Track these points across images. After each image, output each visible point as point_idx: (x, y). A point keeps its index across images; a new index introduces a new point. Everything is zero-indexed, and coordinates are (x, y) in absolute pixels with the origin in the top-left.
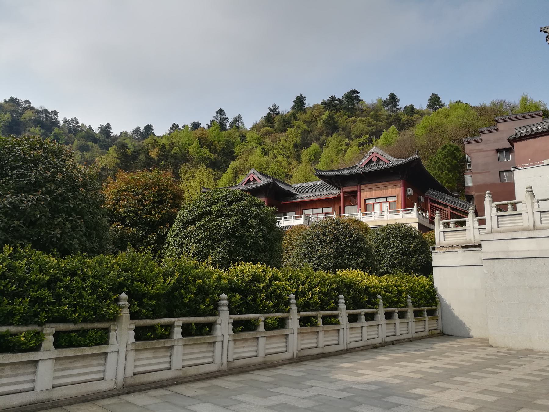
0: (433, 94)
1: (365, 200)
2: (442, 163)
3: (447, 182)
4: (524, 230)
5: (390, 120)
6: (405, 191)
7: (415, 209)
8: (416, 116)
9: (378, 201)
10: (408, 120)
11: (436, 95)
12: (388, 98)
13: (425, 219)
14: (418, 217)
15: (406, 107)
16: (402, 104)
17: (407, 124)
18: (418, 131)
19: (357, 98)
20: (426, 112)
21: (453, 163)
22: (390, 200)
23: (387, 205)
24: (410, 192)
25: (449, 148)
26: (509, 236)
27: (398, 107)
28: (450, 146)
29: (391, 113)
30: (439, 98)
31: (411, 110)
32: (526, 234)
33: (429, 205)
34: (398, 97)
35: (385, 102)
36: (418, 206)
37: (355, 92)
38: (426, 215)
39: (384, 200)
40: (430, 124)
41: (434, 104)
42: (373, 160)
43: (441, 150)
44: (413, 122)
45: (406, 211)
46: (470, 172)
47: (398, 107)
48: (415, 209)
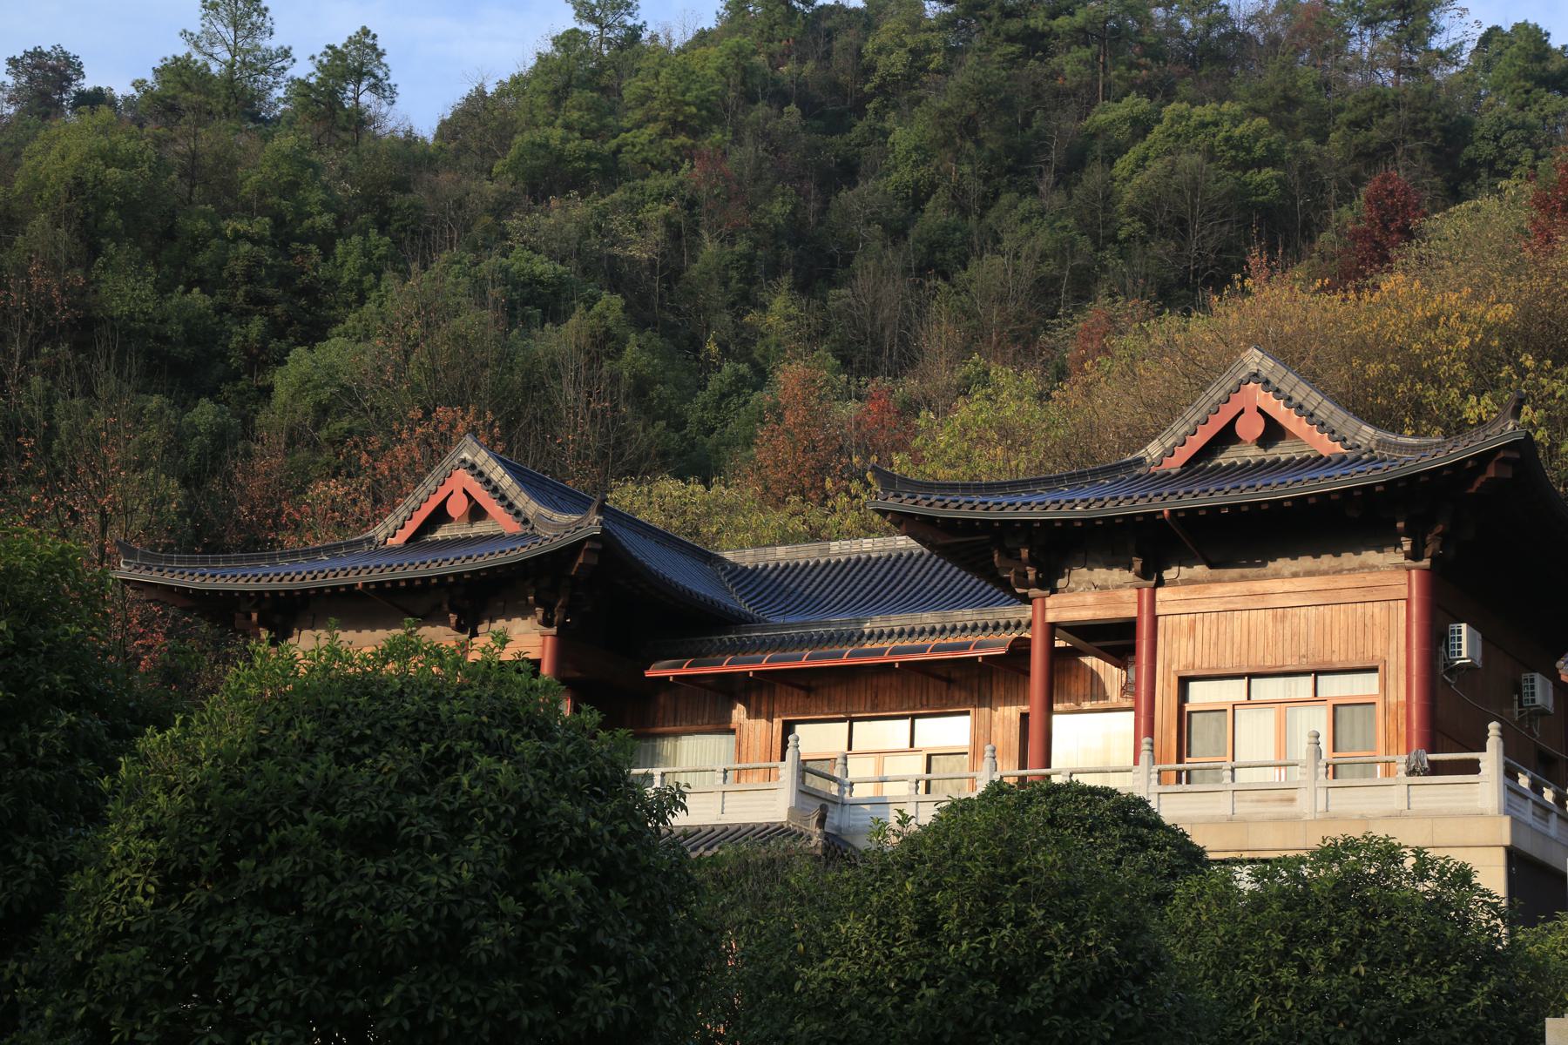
1: (1184, 682)
6: (1436, 639)
7: (1491, 758)
14: (1508, 809)
15: (1492, 36)
22: (1334, 687)
23: (1319, 720)
24: (1465, 643)
27: (1437, 43)
36: (1508, 751)
39: (1303, 686)
42: (1240, 428)
45: (1436, 769)
47: (1437, 43)
48: (1491, 758)
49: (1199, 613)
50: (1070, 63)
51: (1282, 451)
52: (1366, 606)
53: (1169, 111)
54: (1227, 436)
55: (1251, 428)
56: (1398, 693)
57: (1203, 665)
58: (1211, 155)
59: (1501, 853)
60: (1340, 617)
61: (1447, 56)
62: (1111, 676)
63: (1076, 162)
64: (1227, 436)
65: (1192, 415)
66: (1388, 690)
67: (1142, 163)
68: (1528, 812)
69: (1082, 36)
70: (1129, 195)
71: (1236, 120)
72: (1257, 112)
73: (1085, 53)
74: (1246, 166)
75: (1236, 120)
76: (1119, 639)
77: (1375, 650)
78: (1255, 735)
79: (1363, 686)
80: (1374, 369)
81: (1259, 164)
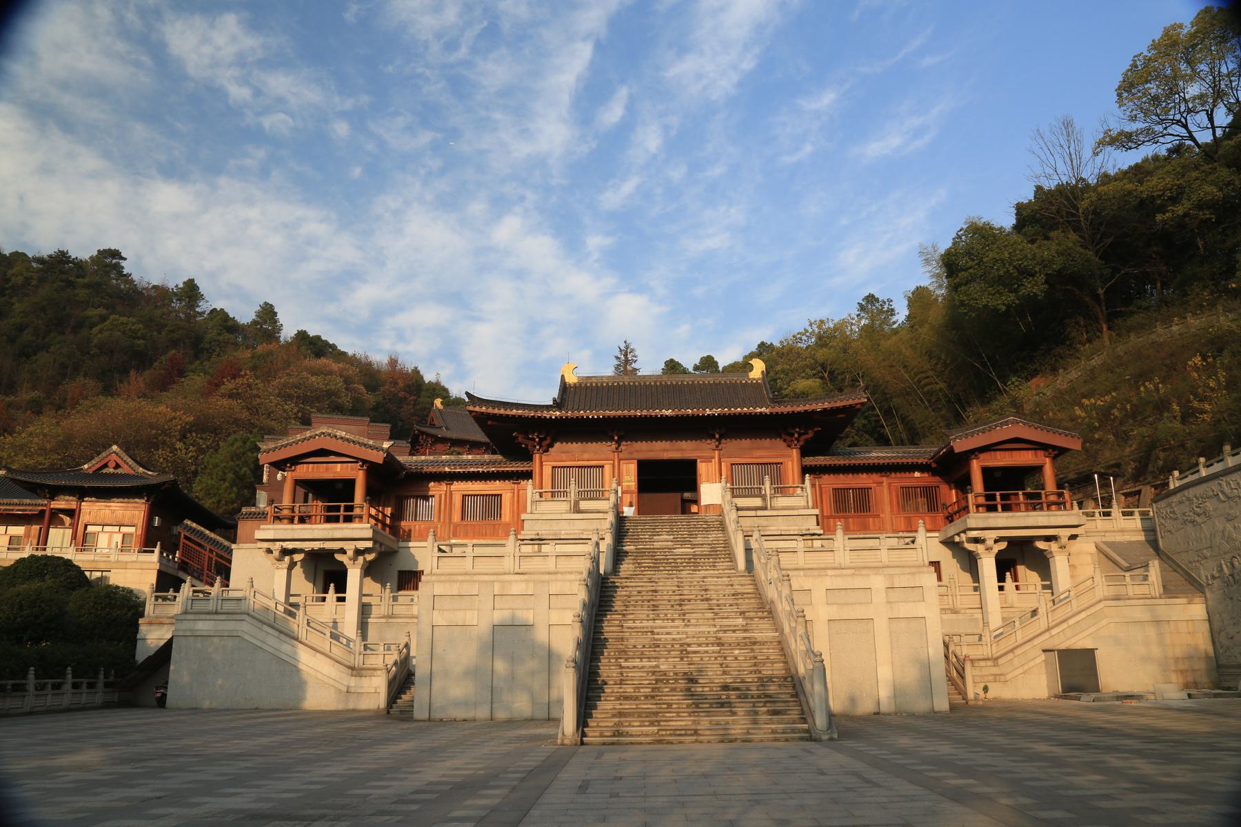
0: (266, 304)
1: (86, 526)
6: (149, 520)
7: (157, 550)
9: (107, 529)
12: (181, 286)
13: (171, 564)
14: (160, 561)
19: (118, 268)
22: (124, 529)
23: (120, 536)
30: (275, 314)
31: (220, 318)
32: (208, 617)
34: (202, 291)
36: (162, 548)
37: (116, 254)
45: (145, 552)
48: (157, 550)
49: (91, 509)
50: (82, 294)
51: (119, 471)
52: (134, 512)
53: (112, 317)
54: (105, 466)
55: (112, 464)
56: (139, 532)
57: (92, 521)
58: (124, 332)
59: (155, 572)
60: (128, 513)
61: (201, 314)
62: (67, 520)
63: (79, 326)
64: (105, 466)
65: (97, 459)
66: (135, 532)
67: (101, 332)
68: (165, 561)
69: (87, 286)
70: (95, 341)
71: (133, 324)
72: (140, 322)
73: (87, 291)
74: (135, 338)
75: (133, 324)
76: (71, 513)
77: (136, 522)
78: (103, 541)
79: (132, 530)
80: (154, 432)
81: (138, 338)
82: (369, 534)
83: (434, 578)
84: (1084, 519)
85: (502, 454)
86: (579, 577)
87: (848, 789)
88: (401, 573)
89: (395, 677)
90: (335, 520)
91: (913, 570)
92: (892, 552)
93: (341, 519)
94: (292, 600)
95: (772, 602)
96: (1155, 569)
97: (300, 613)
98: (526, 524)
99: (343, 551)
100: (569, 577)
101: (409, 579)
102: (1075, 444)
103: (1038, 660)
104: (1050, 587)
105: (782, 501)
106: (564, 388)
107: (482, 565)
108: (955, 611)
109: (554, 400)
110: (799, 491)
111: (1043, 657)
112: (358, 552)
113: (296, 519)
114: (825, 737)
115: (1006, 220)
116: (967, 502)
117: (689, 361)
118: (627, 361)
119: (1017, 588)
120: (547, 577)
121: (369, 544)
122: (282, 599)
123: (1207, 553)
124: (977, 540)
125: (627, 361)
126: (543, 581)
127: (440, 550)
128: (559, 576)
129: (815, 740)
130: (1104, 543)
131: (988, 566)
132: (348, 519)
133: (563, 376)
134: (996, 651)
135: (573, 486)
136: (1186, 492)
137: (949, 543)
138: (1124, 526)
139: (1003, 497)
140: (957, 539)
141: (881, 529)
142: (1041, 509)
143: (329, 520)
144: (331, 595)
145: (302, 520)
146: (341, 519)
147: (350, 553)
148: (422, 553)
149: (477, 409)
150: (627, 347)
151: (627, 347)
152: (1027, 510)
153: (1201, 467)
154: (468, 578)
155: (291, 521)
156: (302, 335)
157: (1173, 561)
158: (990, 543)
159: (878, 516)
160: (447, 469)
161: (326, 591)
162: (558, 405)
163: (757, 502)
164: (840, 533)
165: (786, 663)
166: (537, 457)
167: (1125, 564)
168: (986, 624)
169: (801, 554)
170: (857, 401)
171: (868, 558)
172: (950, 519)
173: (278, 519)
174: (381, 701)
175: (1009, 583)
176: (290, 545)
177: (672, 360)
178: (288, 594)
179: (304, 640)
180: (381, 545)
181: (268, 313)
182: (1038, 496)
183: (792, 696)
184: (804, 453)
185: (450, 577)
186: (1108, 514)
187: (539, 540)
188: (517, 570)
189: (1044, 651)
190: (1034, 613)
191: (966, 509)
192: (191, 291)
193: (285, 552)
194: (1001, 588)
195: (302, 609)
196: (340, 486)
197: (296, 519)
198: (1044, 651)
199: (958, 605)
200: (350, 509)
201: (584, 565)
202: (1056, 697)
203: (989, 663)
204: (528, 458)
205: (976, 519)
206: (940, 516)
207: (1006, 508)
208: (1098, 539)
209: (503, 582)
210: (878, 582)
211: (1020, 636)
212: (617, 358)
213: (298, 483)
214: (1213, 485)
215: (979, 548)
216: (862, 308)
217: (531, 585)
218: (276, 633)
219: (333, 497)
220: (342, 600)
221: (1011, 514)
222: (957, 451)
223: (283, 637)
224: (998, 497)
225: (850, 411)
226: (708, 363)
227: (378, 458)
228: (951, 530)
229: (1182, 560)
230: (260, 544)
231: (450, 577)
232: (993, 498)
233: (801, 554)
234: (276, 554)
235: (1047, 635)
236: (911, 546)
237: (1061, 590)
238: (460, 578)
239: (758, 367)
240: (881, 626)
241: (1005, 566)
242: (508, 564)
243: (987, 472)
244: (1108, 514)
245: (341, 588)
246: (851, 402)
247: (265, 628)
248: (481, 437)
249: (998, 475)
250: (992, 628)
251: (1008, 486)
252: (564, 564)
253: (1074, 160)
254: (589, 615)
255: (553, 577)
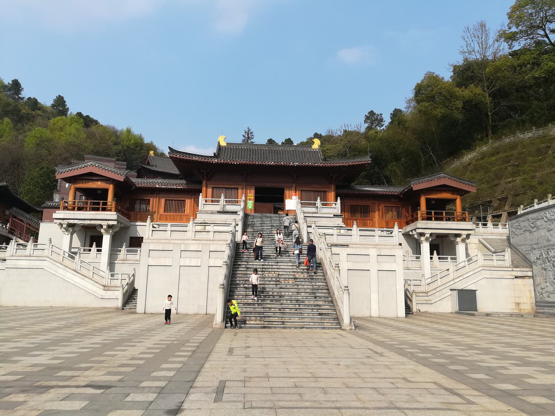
0: (60, 96)
2: (37, 181)
3: (38, 197)
4: (26, 256)
5: (8, 109)
8: (38, 112)
10: (28, 114)
11: (63, 97)
12: (11, 83)
13: (4, 230)
15: (29, 98)
16: (26, 94)
17: (27, 117)
18: (34, 133)
20: (49, 111)
21: (46, 183)
25: (45, 169)
26: (19, 258)
27: (20, 96)
28: (47, 168)
29: (11, 100)
31: (34, 103)
33: (11, 219)
34: (22, 86)
35: (6, 86)
38: (6, 227)
40: (41, 136)
41: (59, 106)
43: (38, 169)
44: (34, 117)
46: (58, 192)
47: (20, 96)
82: (115, 217)
83: (149, 241)
84: (474, 227)
85: (185, 179)
86: (225, 243)
87: (368, 357)
88: (132, 238)
89: (127, 291)
90: (98, 209)
91: (391, 247)
92: (380, 238)
93: (101, 209)
94: (73, 250)
95: (321, 259)
96: (508, 254)
97: (77, 257)
98: (198, 216)
99: (101, 226)
100: (219, 242)
101: (136, 242)
102: (473, 190)
103: (448, 294)
104: (455, 259)
105: (326, 210)
106: (220, 148)
107: (175, 235)
108: (408, 269)
109: (215, 154)
110: (334, 206)
111: (450, 292)
112: (110, 227)
113: (76, 208)
114: (348, 328)
115: (447, 75)
116: (417, 215)
117: (279, 141)
118: (249, 138)
119: (439, 258)
120: (209, 242)
121: (115, 223)
122: (67, 250)
123: (535, 246)
124: (422, 234)
125: (249, 138)
126: (206, 244)
127: (153, 227)
128: (215, 242)
129: (343, 330)
130: (483, 239)
131: (425, 247)
132: (104, 209)
133: (219, 142)
134: (427, 289)
135: (223, 197)
136: (527, 216)
137: (407, 236)
138: (495, 232)
139: (435, 213)
140: (411, 233)
141: (373, 226)
142: (454, 220)
143: (94, 209)
144: (94, 248)
145: (80, 209)
146: (101, 209)
147: (105, 227)
148: (143, 229)
149: (174, 156)
150: (249, 131)
151: (249, 131)
152: (446, 220)
153: (535, 204)
154: (167, 241)
155: (73, 209)
156: (79, 114)
157: (517, 250)
158: (428, 235)
159: (372, 220)
160: (157, 186)
161: (91, 246)
162: (215, 156)
163: (313, 210)
164: (355, 226)
165: (328, 289)
166: (204, 183)
167: (493, 250)
168: (423, 275)
169: (335, 236)
170: (366, 162)
171: (369, 240)
172: (408, 223)
173: (66, 208)
174: (119, 304)
175: (435, 255)
176: (72, 222)
177: (271, 139)
178: (71, 247)
179: (79, 271)
180: (121, 223)
181: (60, 102)
182: (453, 214)
183: (331, 306)
184: (337, 188)
185: (158, 241)
186: (485, 225)
187: (205, 224)
188: (193, 238)
189: (451, 290)
190: (448, 270)
191: (417, 219)
192: (16, 86)
193: (70, 225)
194: (431, 258)
195: (78, 255)
196: (100, 192)
197: (76, 208)
198: (451, 290)
199: (410, 266)
200: (105, 204)
201: (229, 237)
202: (456, 313)
203: (424, 294)
204: (201, 183)
205: (421, 224)
206: (404, 221)
207: (436, 219)
208: (480, 237)
209: (186, 244)
210: (373, 252)
211: (439, 282)
212: (244, 136)
213: (77, 189)
214: (542, 213)
215: (423, 238)
216: (367, 118)
217: (201, 246)
218: (64, 267)
219: (96, 199)
220: (100, 251)
221: (439, 222)
222: (415, 189)
223: (67, 269)
224: (433, 213)
225: (361, 167)
226: (289, 142)
227: (121, 179)
228: (408, 228)
229: (523, 249)
230: (55, 221)
231: (158, 241)
232: (431, 213)
233: (335, 236)
234: (65, 226)
235: (453, 282)
236: (390, 235)
237: (461, 261)
238: (163, 241)
239: (317, 144)
240: (374, 272)
241: (434, 248)
242: (190, 234)
243: (428, 201)
244: (485, 225)
245: (99, 245)
246: (363, 162)
247: (57, 264)
248: (176, 171)
249: (433, 202)
250: (426, 277)
251: (439, 209)
252: (217, 236)
253: (484, 46)
254: (231, 262)
255: (211, 242)
